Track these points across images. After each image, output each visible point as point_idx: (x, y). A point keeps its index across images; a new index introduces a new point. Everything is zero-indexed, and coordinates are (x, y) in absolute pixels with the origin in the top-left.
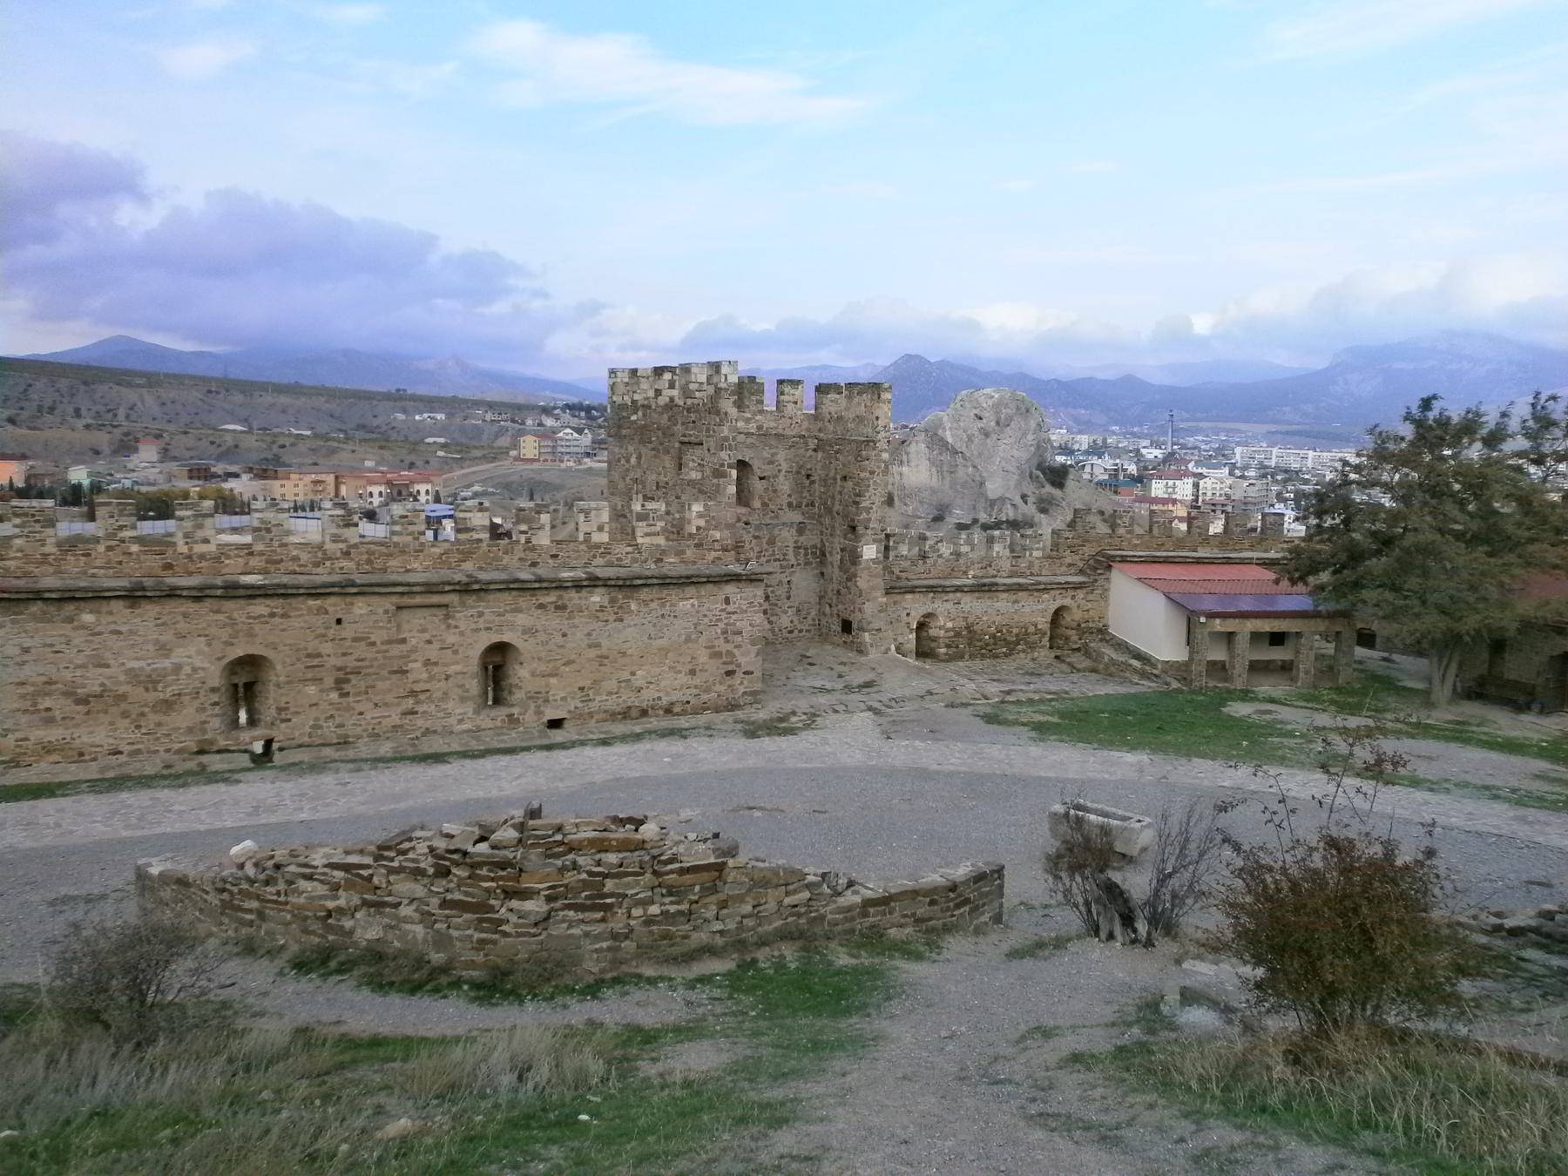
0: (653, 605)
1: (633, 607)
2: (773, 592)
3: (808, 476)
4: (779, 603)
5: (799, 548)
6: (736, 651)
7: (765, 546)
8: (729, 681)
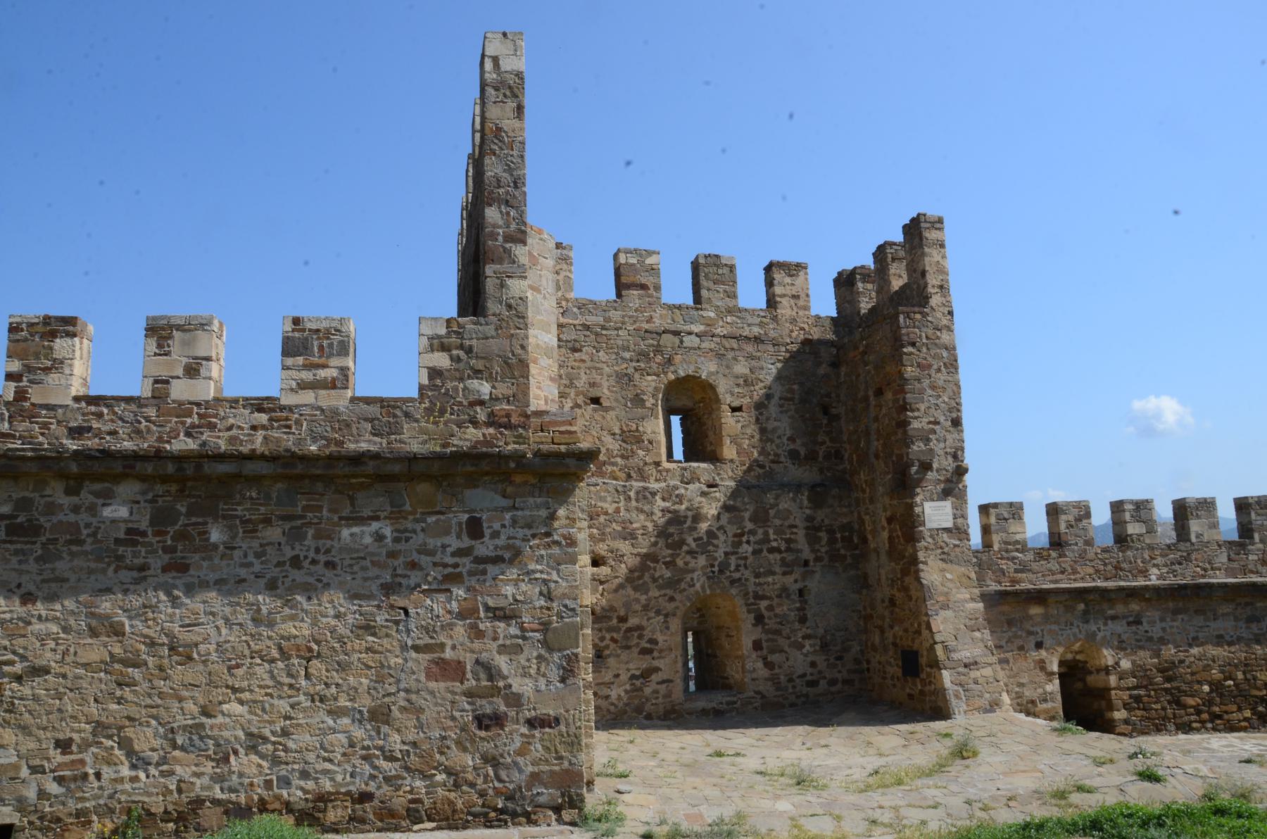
0: (274, 533)
1: (216, 535)
2: (770, 608)
3: (826, 410)
4: (786, 631)
5: (818, 529)
6: (502, 662)
7: (749, 526)
8: (487, 742)
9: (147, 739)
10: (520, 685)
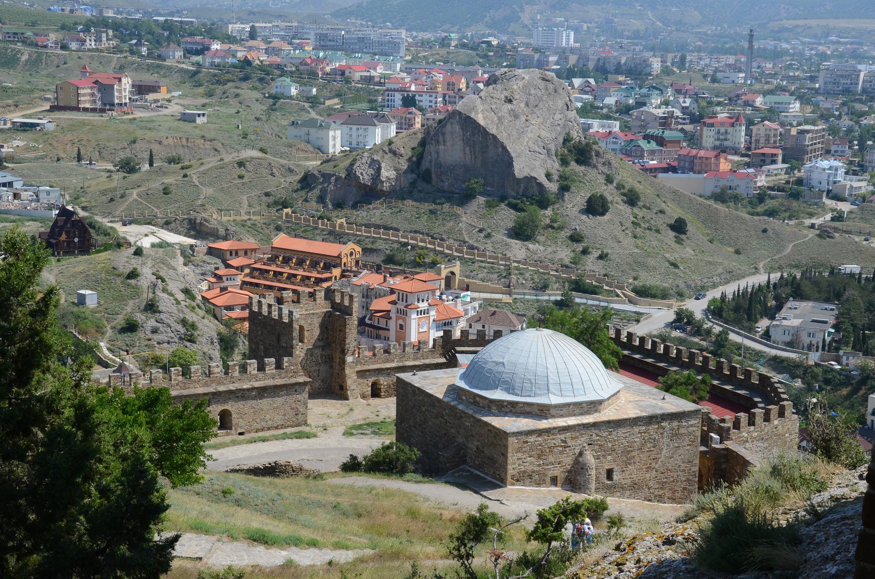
9: (258, 421)
10: (301, 410)
